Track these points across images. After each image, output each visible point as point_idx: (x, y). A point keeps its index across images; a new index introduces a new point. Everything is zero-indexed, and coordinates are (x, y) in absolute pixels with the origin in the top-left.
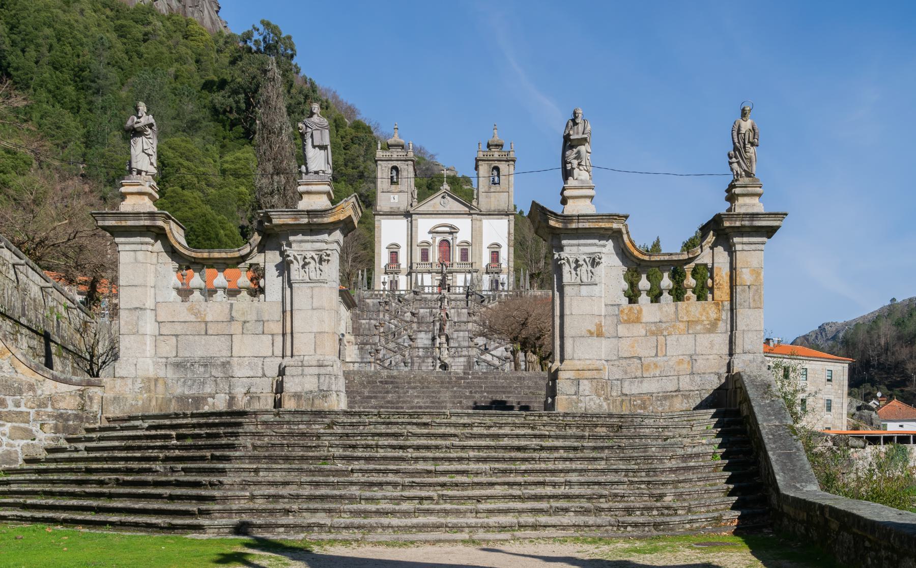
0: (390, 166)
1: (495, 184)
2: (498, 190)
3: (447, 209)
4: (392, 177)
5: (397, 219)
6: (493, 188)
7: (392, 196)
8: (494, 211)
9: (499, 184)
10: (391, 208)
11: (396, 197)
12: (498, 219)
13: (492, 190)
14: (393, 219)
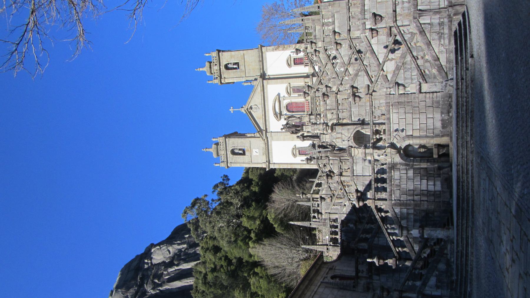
0: (231, 156)
1: (239, 68)
2: (243, 64)
3: (260, 106)
4: (240, 154)
5: (272, 150)
6: (242, 67)
7: (254, 153)
8: (260, 65)
9: (237, 64)
10: (263, 154)
11: (254, 151)
12: (266, 62)
13: (244, 69)
14: (272, 153)
